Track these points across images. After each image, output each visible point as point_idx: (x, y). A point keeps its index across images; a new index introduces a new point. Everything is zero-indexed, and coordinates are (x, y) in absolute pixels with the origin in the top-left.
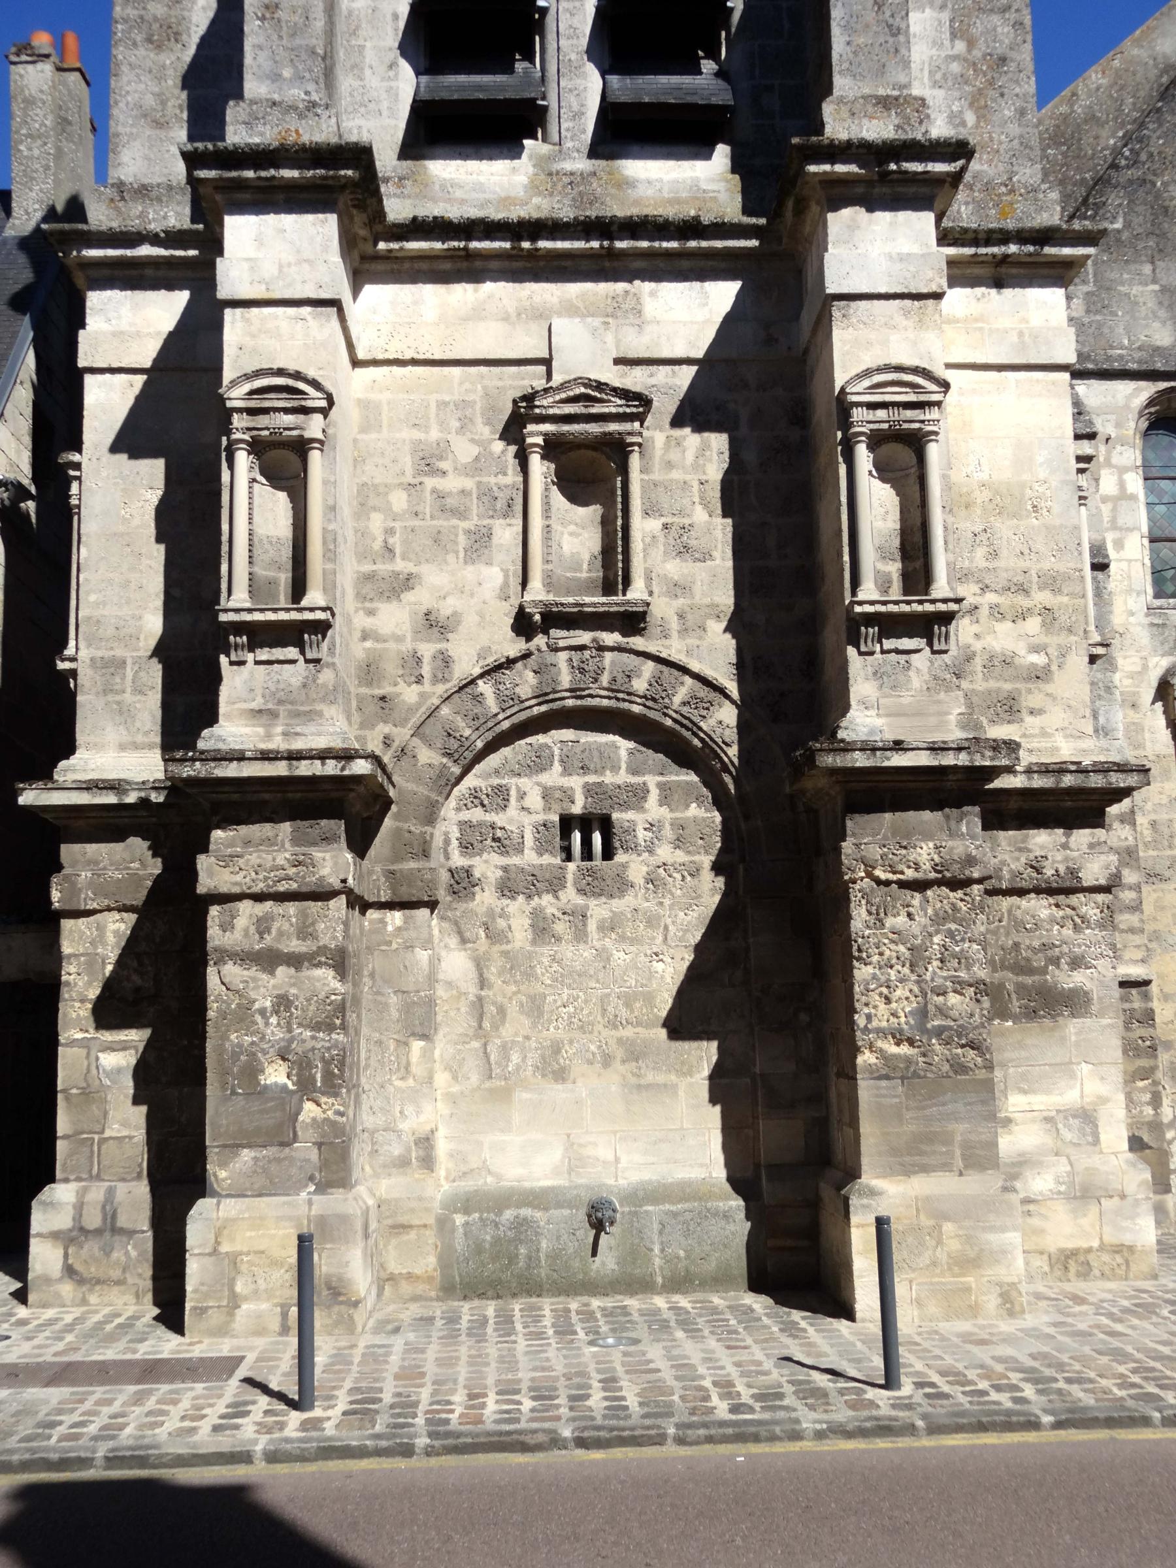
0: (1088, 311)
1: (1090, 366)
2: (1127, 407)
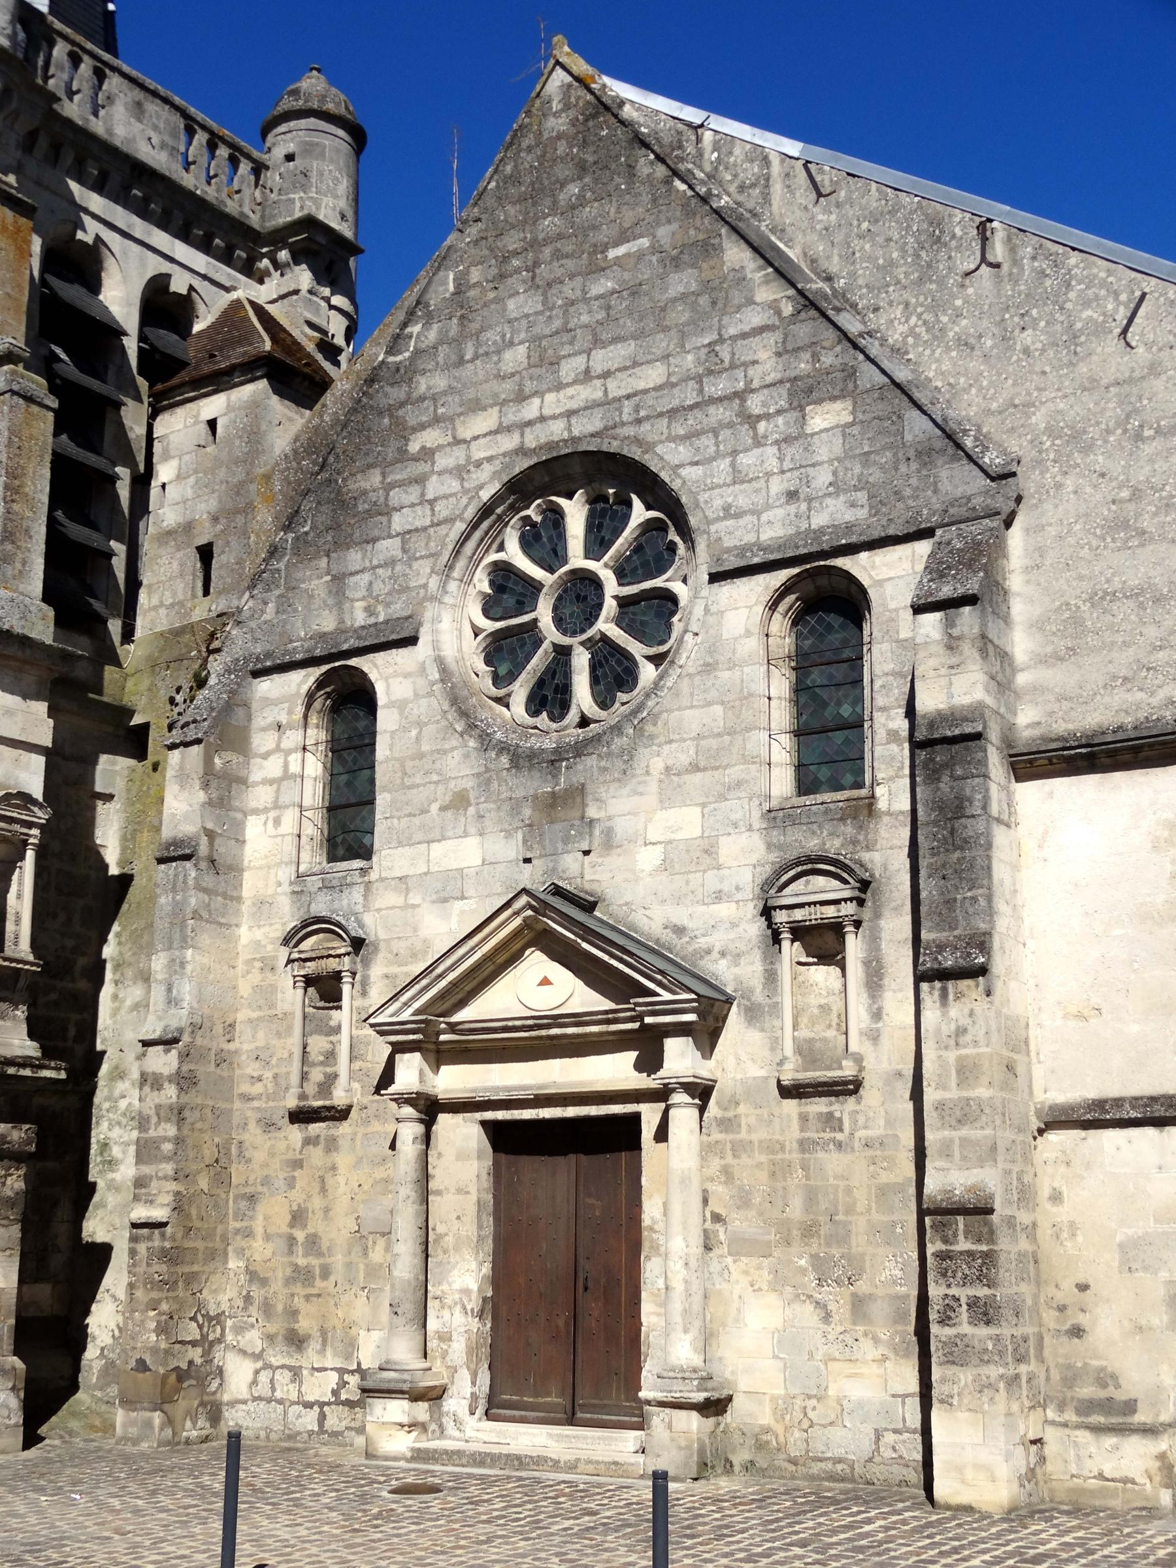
0: (277, 612)
1: (268, 664)
2: (298, 693)
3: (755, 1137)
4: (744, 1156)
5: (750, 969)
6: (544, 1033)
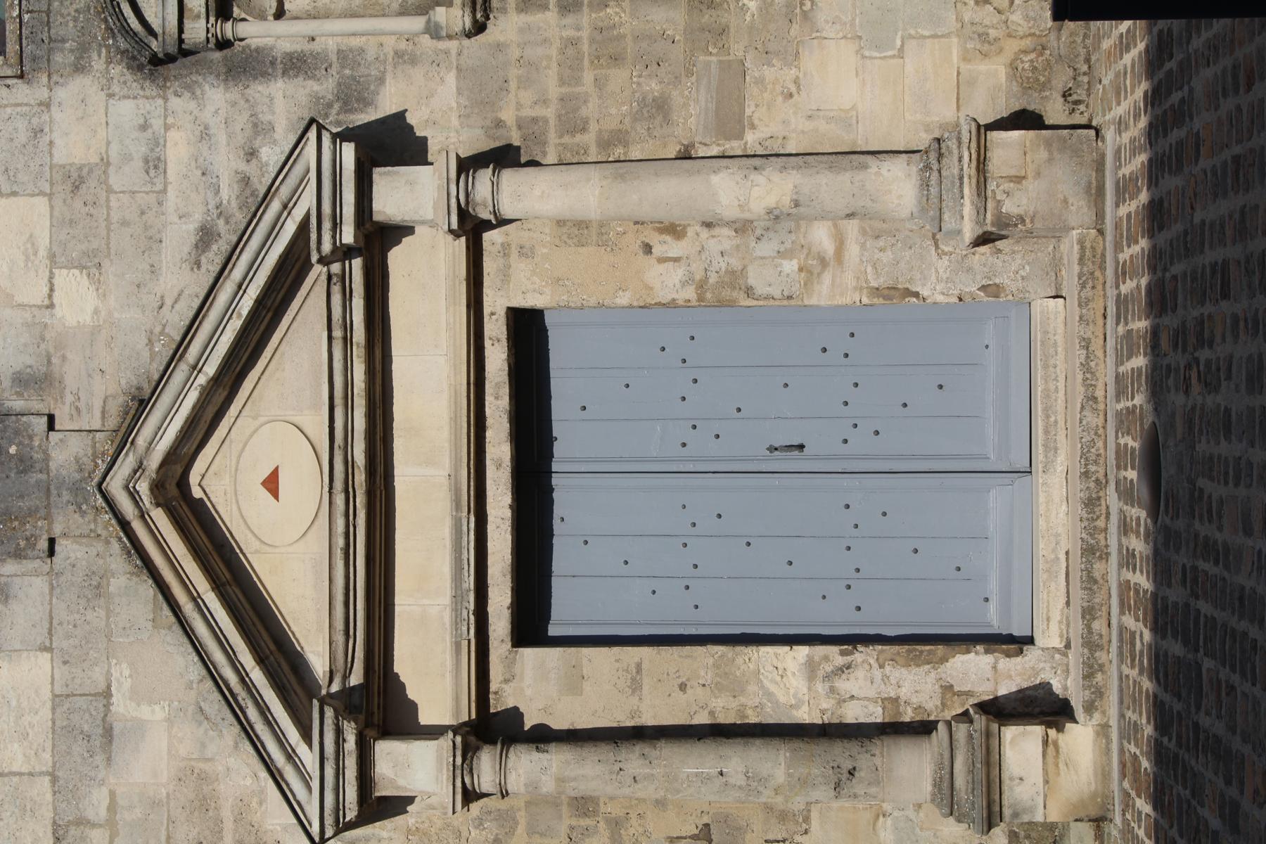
3: (554, 90)
4: (584, 112)
5: (280, 105)
6: (360, 478)
